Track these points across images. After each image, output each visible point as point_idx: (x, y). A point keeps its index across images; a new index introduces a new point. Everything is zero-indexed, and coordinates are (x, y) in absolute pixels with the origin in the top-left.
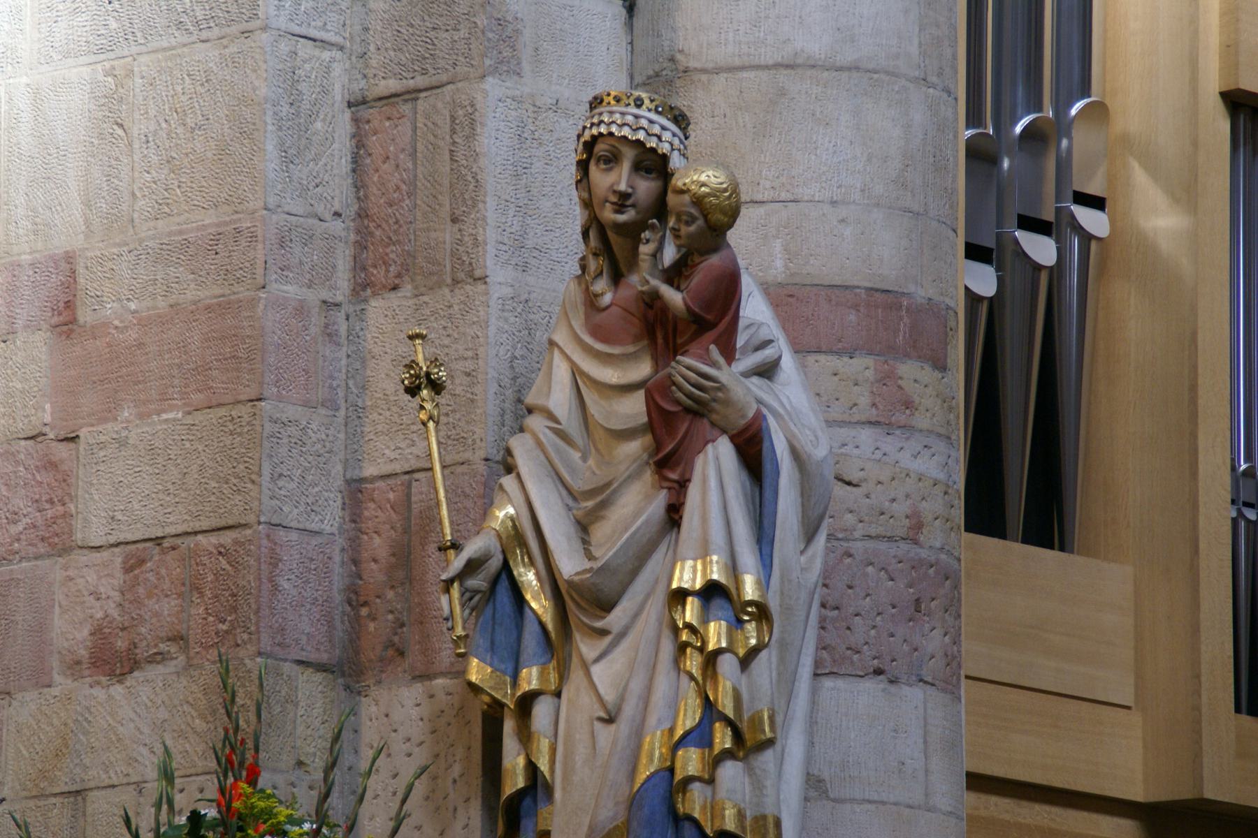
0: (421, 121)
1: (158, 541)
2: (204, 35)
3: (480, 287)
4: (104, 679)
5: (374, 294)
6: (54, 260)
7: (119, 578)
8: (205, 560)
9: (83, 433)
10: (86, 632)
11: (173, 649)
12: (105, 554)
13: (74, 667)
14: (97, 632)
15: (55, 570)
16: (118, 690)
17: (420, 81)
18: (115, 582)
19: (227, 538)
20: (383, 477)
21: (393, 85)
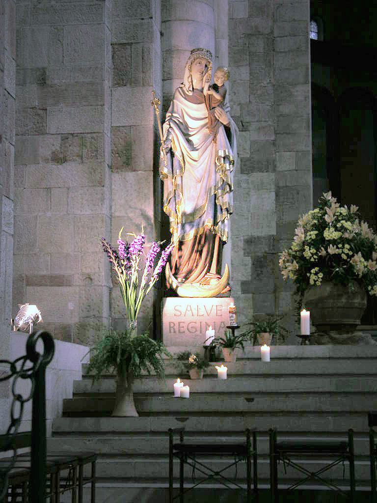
0: (133, 50)
1: (72, 134)
2: (85, 23)
3: (151, 87)
4: (56, 164)
5: (119, 86)
6: (38, 69)
7: (60, 141)
8: (88, 139)
9: (48, 108)
10: (50, 153)
11: (77, 158)
12: (56, 136)
13: (46, 160)
14: (53, 153)
15: (41, 138)
16: (60, 166)
17: (133, 41)
18: (59, 142)
19: (94, 135)
20: (123, 127)
21: (125, 41)
